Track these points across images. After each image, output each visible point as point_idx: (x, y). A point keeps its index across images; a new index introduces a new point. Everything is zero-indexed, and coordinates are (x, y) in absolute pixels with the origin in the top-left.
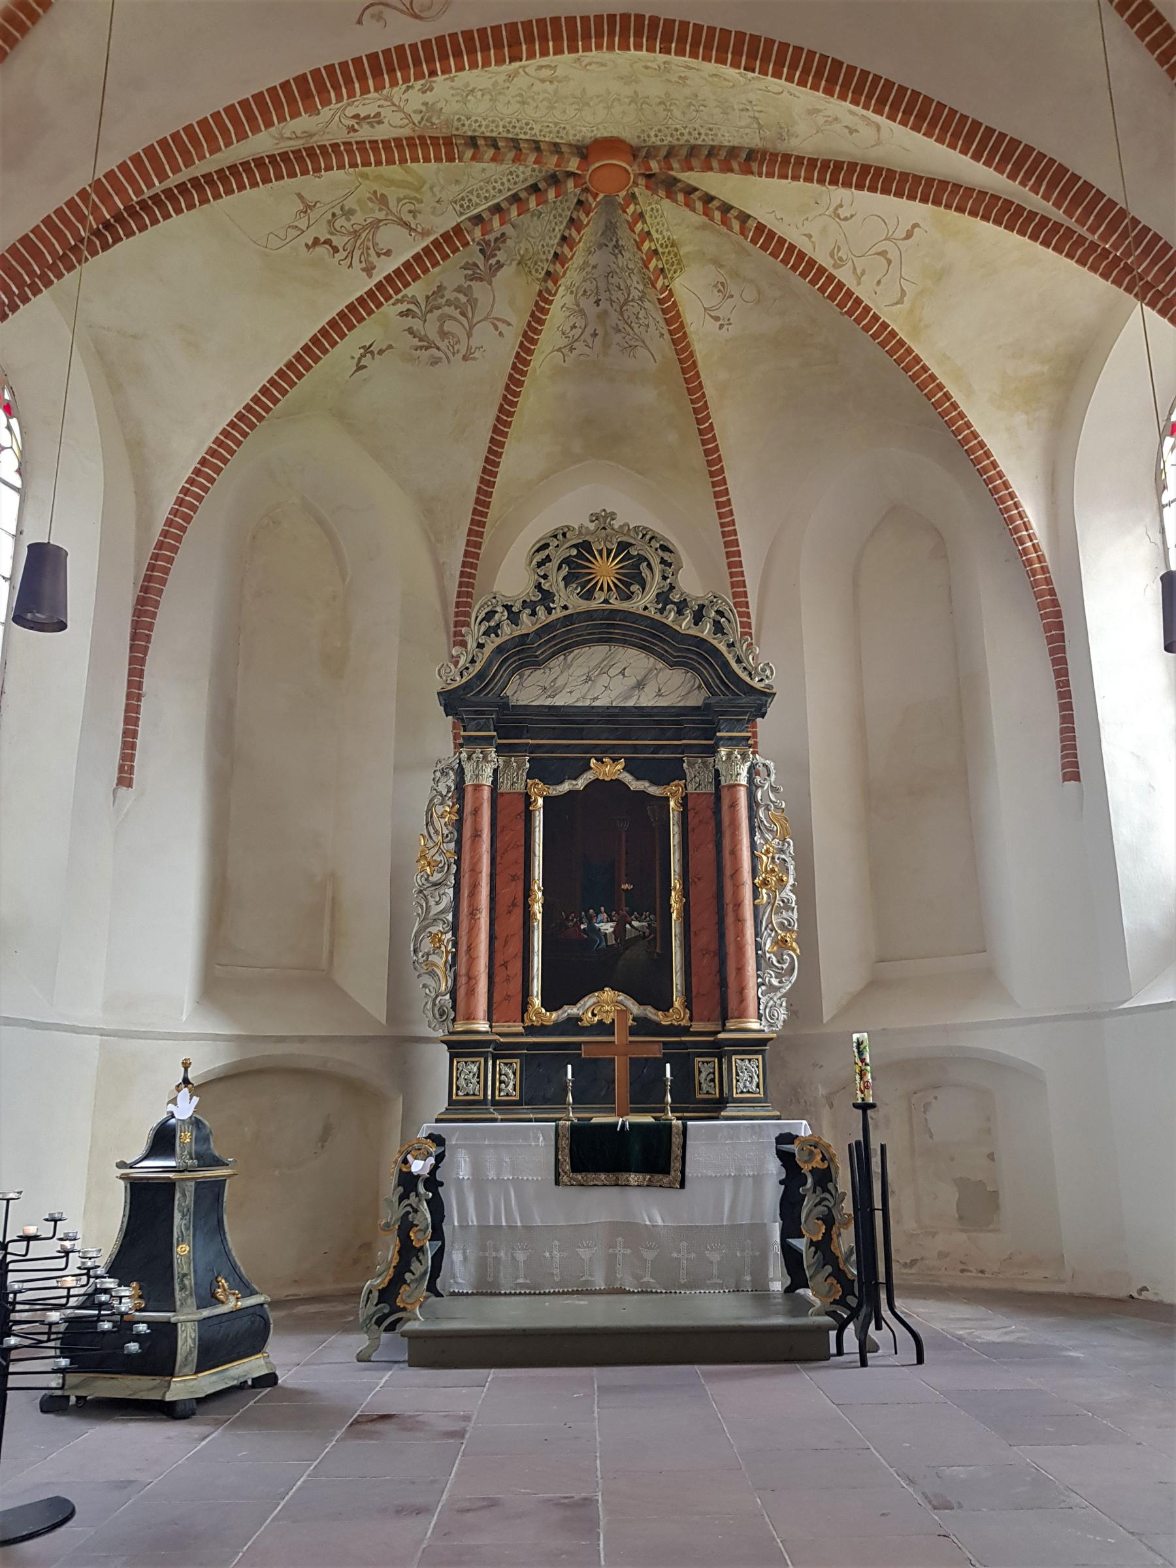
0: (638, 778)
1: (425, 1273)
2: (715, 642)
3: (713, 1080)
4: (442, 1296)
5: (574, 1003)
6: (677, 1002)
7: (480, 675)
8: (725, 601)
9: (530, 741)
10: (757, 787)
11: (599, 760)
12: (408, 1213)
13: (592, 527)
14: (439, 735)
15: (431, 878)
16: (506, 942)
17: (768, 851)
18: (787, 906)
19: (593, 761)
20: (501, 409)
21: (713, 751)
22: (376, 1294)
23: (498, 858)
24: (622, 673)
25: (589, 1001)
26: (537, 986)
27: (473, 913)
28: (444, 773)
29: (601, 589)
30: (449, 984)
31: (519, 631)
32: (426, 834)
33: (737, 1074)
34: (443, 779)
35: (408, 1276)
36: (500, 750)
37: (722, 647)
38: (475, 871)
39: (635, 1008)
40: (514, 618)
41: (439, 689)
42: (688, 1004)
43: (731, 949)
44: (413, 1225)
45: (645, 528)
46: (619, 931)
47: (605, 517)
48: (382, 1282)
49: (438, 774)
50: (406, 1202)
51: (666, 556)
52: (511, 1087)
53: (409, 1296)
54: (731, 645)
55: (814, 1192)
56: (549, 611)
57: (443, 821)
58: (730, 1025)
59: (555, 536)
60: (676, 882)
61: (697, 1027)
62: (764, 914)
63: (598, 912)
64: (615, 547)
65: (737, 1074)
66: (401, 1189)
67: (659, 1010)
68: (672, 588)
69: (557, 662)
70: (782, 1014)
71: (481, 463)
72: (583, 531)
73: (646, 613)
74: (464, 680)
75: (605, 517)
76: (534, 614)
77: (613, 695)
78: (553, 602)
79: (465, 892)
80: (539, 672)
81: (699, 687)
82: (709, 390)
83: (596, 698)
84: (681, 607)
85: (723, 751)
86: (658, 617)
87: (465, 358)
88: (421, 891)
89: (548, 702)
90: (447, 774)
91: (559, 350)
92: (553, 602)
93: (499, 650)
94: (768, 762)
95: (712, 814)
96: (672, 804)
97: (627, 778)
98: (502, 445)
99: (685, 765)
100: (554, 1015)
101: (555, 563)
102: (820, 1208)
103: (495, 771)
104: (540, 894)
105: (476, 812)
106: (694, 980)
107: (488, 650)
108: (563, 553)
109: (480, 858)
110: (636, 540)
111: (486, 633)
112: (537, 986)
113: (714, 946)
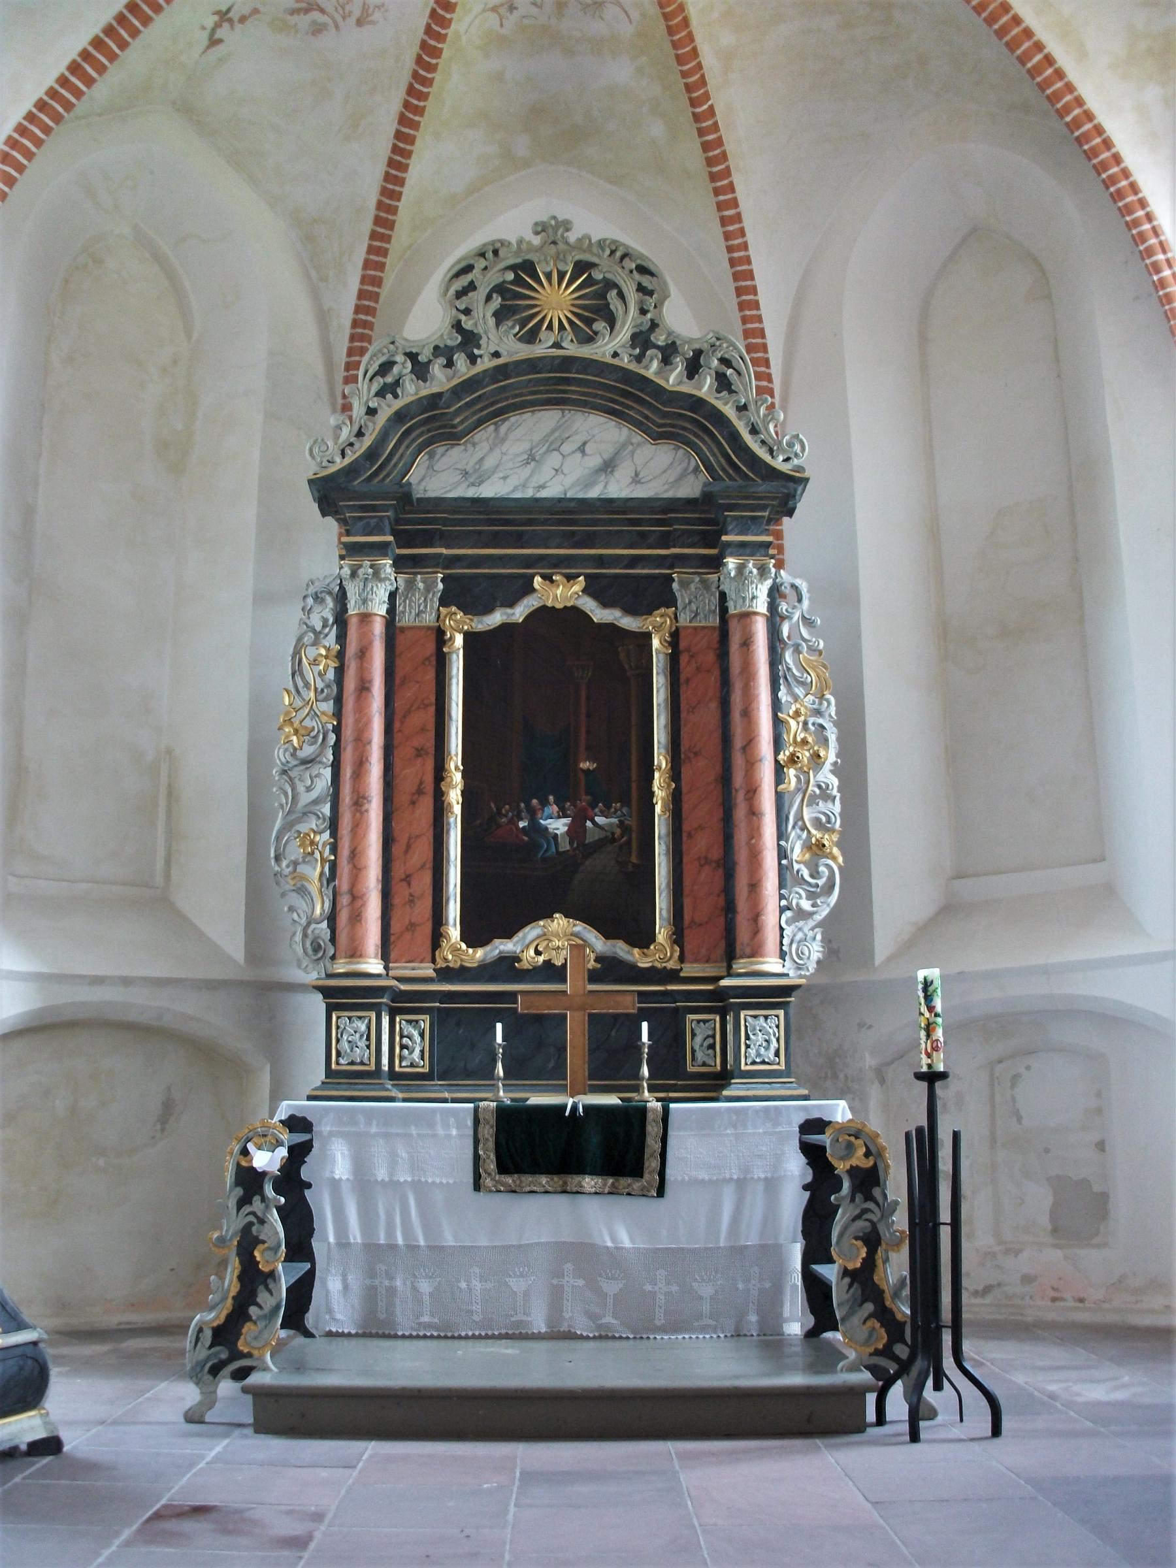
0: (605, 604)
1: (278, 1307)
2: (719, 404)
3: (712, 1046)
5: (509, 935)
6: (662, 934)
7: (371, 454)
9: (444, 551)
10: (783, 618)
11: (547, 578)
16: (409, 846)
17: (797, 713)
18: (825, 794)
19: (538, 580)
20: (411, 91)
21: (716, 564)
22: (208, 1335)
23: (397, 725)
24: (582, 449)
25: (531, 932)
26: (454, 910)
27: (360, 801)
28: (317, 598)
29: (550, 327)
30: (327, 905)
32: (292, 689)
33: (748, 1038)
35: (253, 1311)
36: (400, 564)
37: (729, 411)
38: (362, 741)
39: (598, 943)
40: (421, 371)
42: (678, 937)
43: (742, 856)
44: (257, 1241)
45: (614, 242)
46: (576, 831)
49: (310, 601)
50: (247, 1209)
51: (646, 281)
53: (256, 1338)
54: (742, 409)
55: (853, 1200)
56: (473, 359)
58: (740, 966)
59: (483, 255)
60: (661, 759)
61: (689, 970)
62: (791, 806)
63: (544, 803)
65: (748, 1038)
66: (239, 1191)
67: (634, 945)
68: (654, 325)
69: (485, 434)
70: (815, 951)
71: (380, 168)
72: (524, 246)
73: (616, 362)
74: (347, 461)
76: (450, 364)
77: (568, 481)
78: (479, 347)
79: (347, 772)
81: (696, 470)
82: (709, 59)
83: (542, 487)
84: (668, 353)
85: (731, 563)
86: (633, 367)
87: (360, 23)
89: (471, 493)
90: (323, 600)
91: (494, 9)
92: (479, 347)
93: (399, 417)
94: (798, 582)
96: (656, 643)
97: (589, 605)
98: (411, 140)
99: (675, 586)
100: (480, 953)
102: (860, 1224)
103: (392, 596)
104: (457, 777)
105: (363, 653)
106: (687, 902)
107: (382, 418)
108: (495, 277)
109: (368, 723)
111: (381, 394)
112: (454, 910)
113: (716, 853)
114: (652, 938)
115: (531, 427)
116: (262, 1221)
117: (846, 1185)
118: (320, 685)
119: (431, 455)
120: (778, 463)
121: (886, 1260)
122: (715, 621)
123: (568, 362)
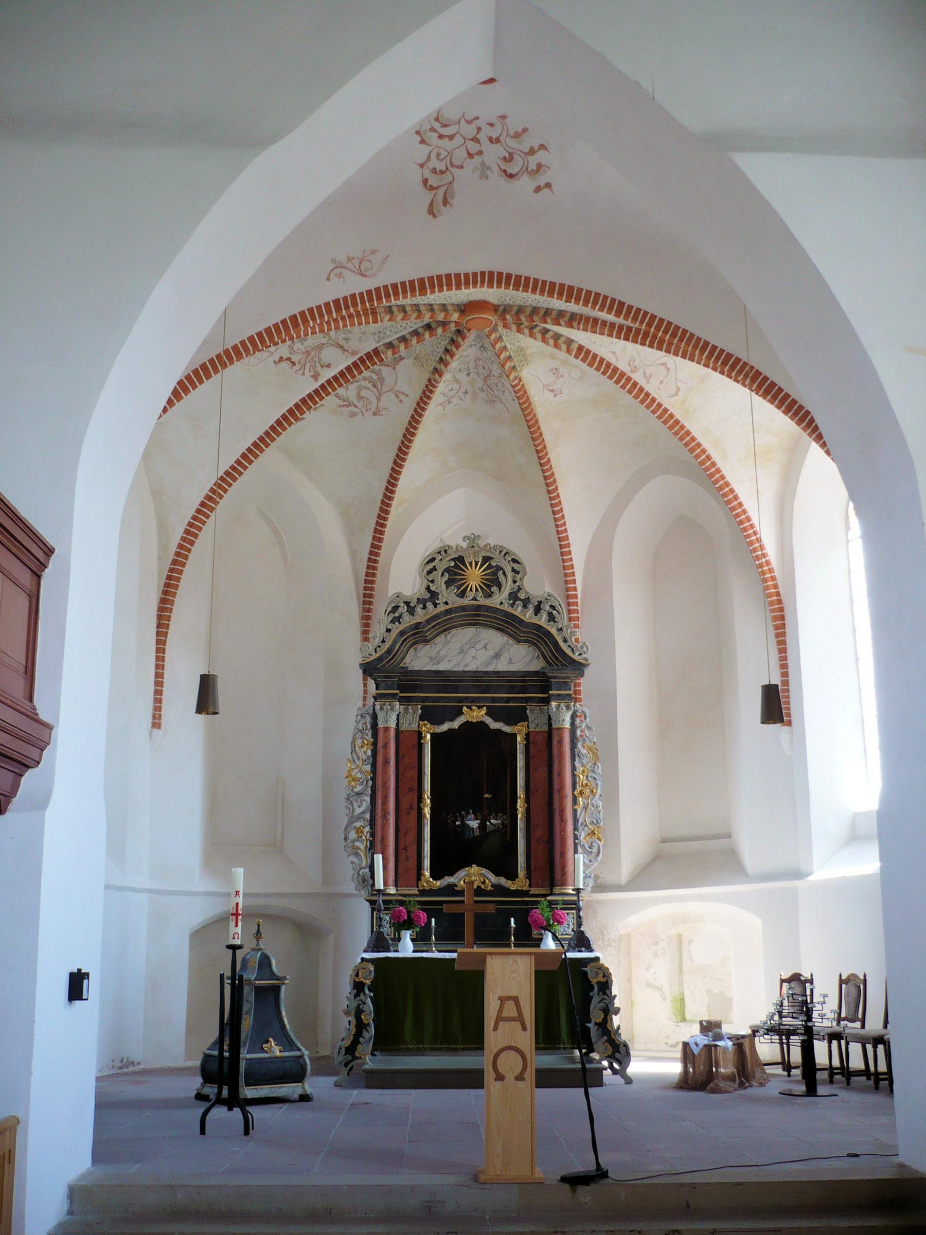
0: (496, 720)
2: (548, 628)
5: (452, 874)
6: (521, 872)
7: (389, 652)
8: (556, 598)
11: (469, 707)
13: (464, 545)
17: (583, 771)
20: (400, 449)
21: (547, 701)
22: (343, 1050)
24: (485, 647)
25: (462, 873)
27: (385, 815)
29: (471, 590)
30: (369, 861)
35: (361, 1040)
37: (554, 631)
38: (385, 786)
40: (411, 611)
42: (529, 876)
46: (482, 826)
49: (359, 717)
56: (435, 605)
57: (362, 750)
58: (557, 890)
59: (439, 553)
60: (521, 793)
61: (533, 891)
63: (468, 813)
67: (508, 879)
68: (519, 589)
69: (440, 640)
71: (385, 484)
73: (501, 607)
74: (378, 655)
76: (425, 607)
79: (379, 801)
82: (547, 436)
83: (466, 665)
85: (554, 704)
86: (510, 610)
87: (374, 414)
89: (434, 668)
91: (441, 404)
93: (402, 633)
95: (546, 747)
96: (519, 739)
97: (488, 720)
98: (399, 473)
100: (438, 883)
104: (429, 801)
105: (386, 746)
109: (389, 778)
111: (392, 622)
112: (427, 863)
114: (517, 876)
115: (463, 635)
116: (364, 1003)
117: (596, 988)
118: (365, 757)
119: (415, 649)
120: (576, 657)
122: (547, 729)
123: (479, 607)
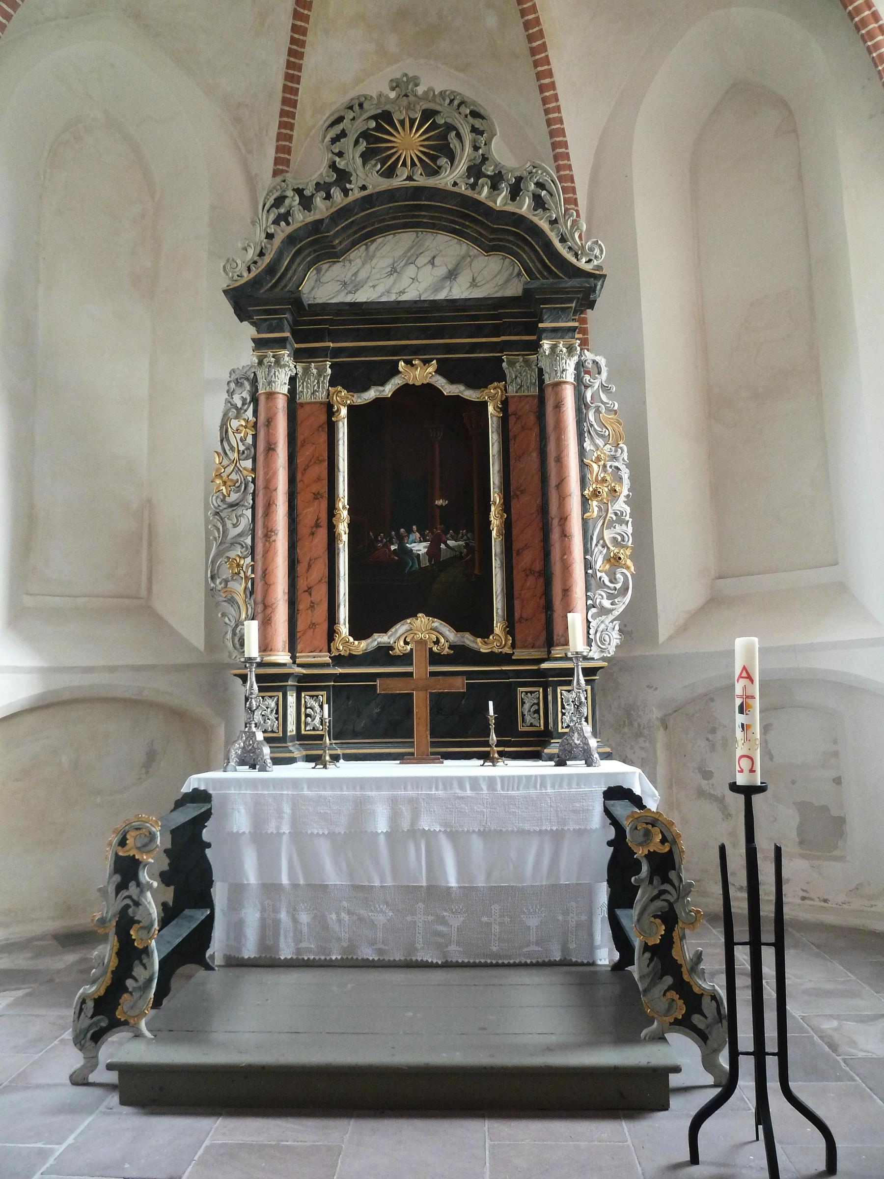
0: (452, 381)
1: (150, 980)
2: (535, 220)
3: (537, 712)
4: (212, 969)
5: (384, 630)
6: (498, 627)
7: (271, 269)
8: (545, 171)
9: (331, 345)
10: (586, 387)
11: (409, 363)
12: (127, 907)
13: (393, 95)
14: (234, 345)
15: (227, 499)
16: (309, 566)
17: (598, 459)
18: (620, 519)
19: (402, 364)
21: (535, 347)
22: (90, 1004)
23: (299, 476)
24: (432, 262)
25: (401, 629)
26: (343, 613)
27: (269, 534)
28: (238, 383)
29: (404, 164)
31: (311, 217)
32: (220, 450)
33: (563, 707)
34: (238, 390)
35: (130, 983)
36: (298, 356)
37: (544, 225)
39: (449, 635)
40: (306, 203)
41: (224, 286)
43: (557, 569)
44: (132, 922)
45: (452, 92)
46: (433, 552)
47: (408, 82)
48: (98, 989)
49: (233, 385)
50: (124, 893)
51: (477, 123)
52: (317, 721)
53: (132, 1007)
54: (554, 222)
55: (651, 882)
56: (346, 192)
57: (238, 436)
58: (557, 652)
59: (351, 108)
60: (496, 496)
61: (519, 654)
62: (594, 528)
63: (409, 531)
64: (418, 116)
65: (563, 707)
66: (117, 878)
69: (358, 254)
70: (615, 638)
71: (283, 58)
72: (383, 99)
73: (456, 189)
74: (252, 275)
75: (408, 82)
76: (328, 197)
77: (422, 286)
78: (350, 182)
80: (338, 266)
81: (519, 274)
83: (403, 292)
84: (496, 181)
85: (546, 344)
86: (469, 193)
88: (217, 513)
89: (349, 299)
90: (242, 385)
92: (350, 182)
93: (291, 239)
94: (598, 358)
95: (534, 421)
96: (491, 409)
97: (440, 382)
99: (504, 365)
101: (352, 138)
102: (658, 904)
103: (293, 380)
104: (345, 514)
106: (517, 603)
107: (277, 241)
108: (360, 126)
109: (275, 473)
110: (442, 106)
111: (276, 222)
112: (343, 613)
113: (538, 566)
114: (491, 631)
115: (391, 247)
116: (137, 904)
117: (645, 868)
118: (242, 448)
119: (318, 271)
120: (582, 264)
121: (683, 938)
122: (535, 391)
123: (419, 192)
